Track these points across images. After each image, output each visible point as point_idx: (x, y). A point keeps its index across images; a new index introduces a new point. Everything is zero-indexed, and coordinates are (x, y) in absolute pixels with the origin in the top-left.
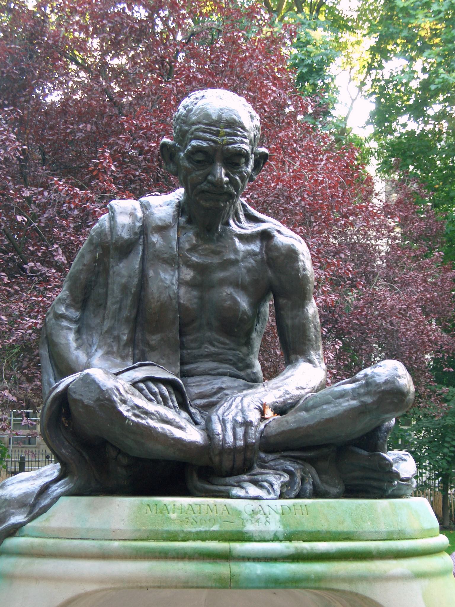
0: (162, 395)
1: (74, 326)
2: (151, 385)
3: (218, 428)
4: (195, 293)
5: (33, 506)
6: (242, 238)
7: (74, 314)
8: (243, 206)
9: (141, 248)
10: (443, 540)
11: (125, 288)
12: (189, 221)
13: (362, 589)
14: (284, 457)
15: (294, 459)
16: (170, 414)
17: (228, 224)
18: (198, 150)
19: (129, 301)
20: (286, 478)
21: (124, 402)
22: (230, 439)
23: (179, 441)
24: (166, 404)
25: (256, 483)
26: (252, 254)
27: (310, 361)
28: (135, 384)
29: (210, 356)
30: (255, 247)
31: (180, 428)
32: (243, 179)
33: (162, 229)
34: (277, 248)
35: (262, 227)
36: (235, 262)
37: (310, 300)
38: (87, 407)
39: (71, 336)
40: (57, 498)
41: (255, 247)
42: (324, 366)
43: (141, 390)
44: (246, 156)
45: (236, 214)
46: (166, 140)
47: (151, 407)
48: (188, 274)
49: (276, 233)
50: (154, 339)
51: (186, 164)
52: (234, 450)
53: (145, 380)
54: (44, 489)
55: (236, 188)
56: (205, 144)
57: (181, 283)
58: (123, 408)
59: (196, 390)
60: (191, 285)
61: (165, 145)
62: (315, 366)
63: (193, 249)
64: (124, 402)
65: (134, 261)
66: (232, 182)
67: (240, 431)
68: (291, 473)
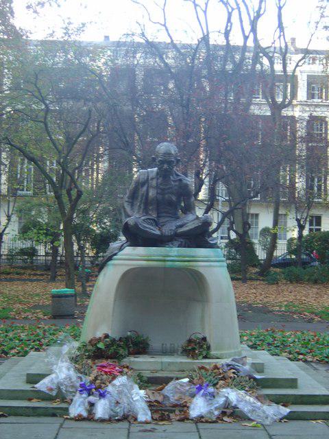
6: (173, 181)
7: (130, 201)
15: (183, 239)
16: (152, 227)
19: (144, 198)
20: (180, 243)
26: (176, 185)
28: (144, 220)
29: (165, 212)
30: (177, 183)
33: (152, 179)
36: (171, 188)
41: (177, 183)
44: (173, 161)
50: (151, 208)
51: (158, 163)
57: (157, 193)
63: (161, 184)
65: (145, 188)
68: (181, 242)
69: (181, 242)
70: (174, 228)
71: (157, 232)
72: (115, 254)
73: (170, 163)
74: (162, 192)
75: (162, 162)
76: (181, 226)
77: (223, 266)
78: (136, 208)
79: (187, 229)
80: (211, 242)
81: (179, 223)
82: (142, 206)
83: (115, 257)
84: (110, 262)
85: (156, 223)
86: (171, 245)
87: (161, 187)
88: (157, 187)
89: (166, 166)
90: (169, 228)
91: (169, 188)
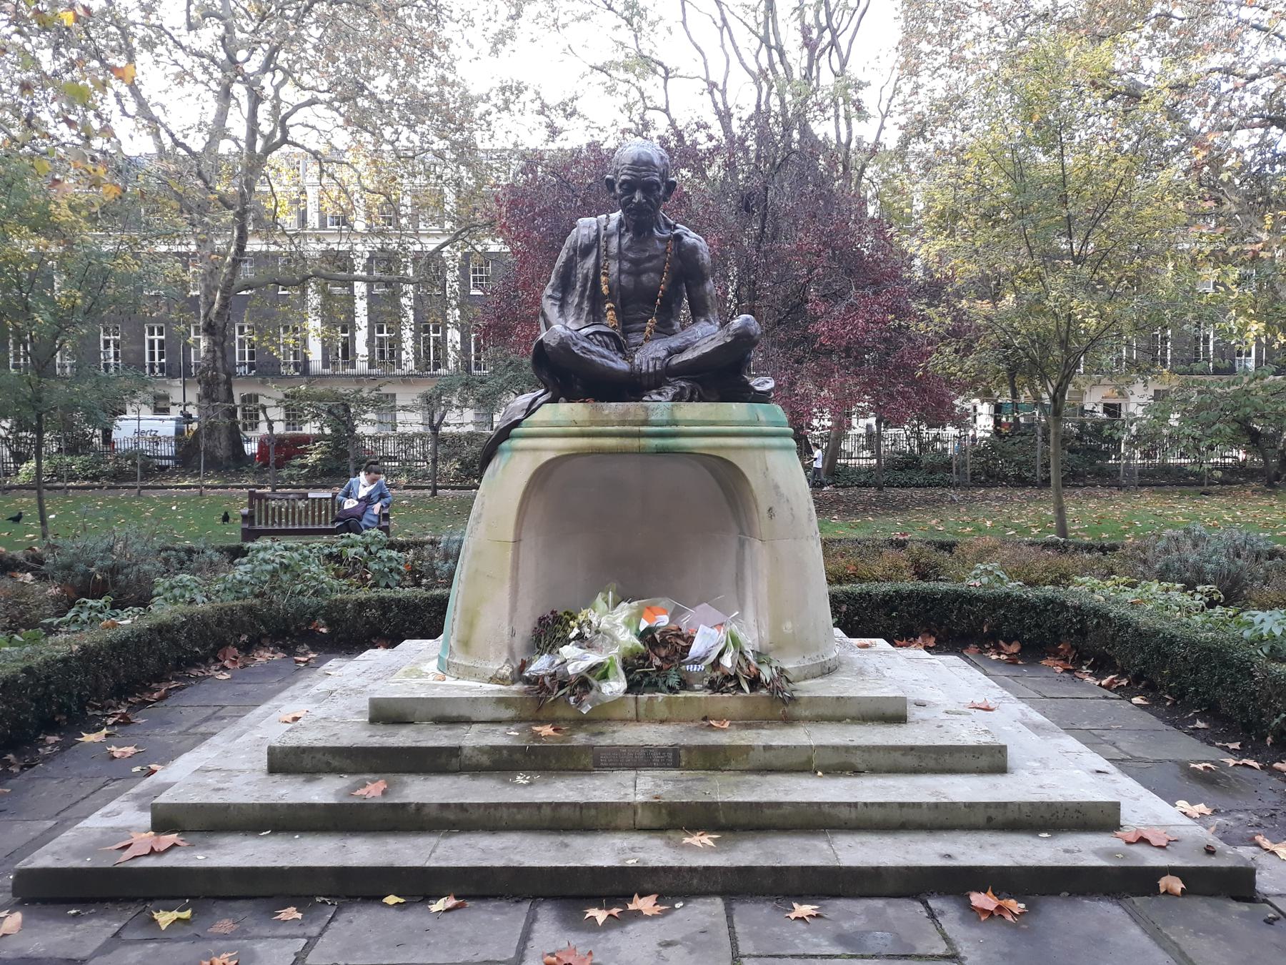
0: (606, 343)
1: (558, 303)
2: (598, 336)
3: (637, 362)
4: (630, 278)
5: (528, 410)
8: (664, 218)
9: (596, 250)
10: (791, 430)
11: (586, 277)
12: (627, 230)
13: (723, 454)
14: (681, 379)
15: (687, 380)
16: (606, 352)
17: (652, 231)
18: (625, 182)
21: (576, 344)
22: (644, 368)
23: (611, 368)
24: (607, 347)
25: (660, 394)
27: (708, 321)
28: (587, 336)
31: (613, 361)
32: (656, 200)
34: (684, 245)
35: (677, 231)
36: (656, 257)
37: (708, 280)
38: (552, 347)
39: (556, 309)
40: (540, 406)
42: (718, 323)
43: (591, 340)
44: (657, 184)
45: (659, 224)
46: (608, 176)
47: (594, 348)
48: (626, 265)
49: (685, 237)
52: (647, 373)
53: (593, 334)
54: (535, 400)
55: (652, 206)
56: (629, 178)
58: (575, 349)
59: (633, 341)
60: (629, 273)
61: (608, 179)
62: (711, 324)
63: (629, 249)
64: (576, 344)
65: (591, 261)
66: (649, 202)
67: (651, 364)
69: (682, 388)
70: (663, 354)
71: (621, 365)
72: (517, 423)
73: (648, 188)
74: (637, 269)
75: (630, 187)
76: (681, 351)
77: (787, 448)
78: (571, 310)
79: (696, 354)
80: (758, 388)
81: (675, 342)
82: (586, 306)
83: (516, 431)
84: (505, 444)
85: (622, 348)
86: (655, 397)
87: (631, 255)
88: (620, 256)
89: (638, 196)
90: (651, 353)
91: (650, 258)
